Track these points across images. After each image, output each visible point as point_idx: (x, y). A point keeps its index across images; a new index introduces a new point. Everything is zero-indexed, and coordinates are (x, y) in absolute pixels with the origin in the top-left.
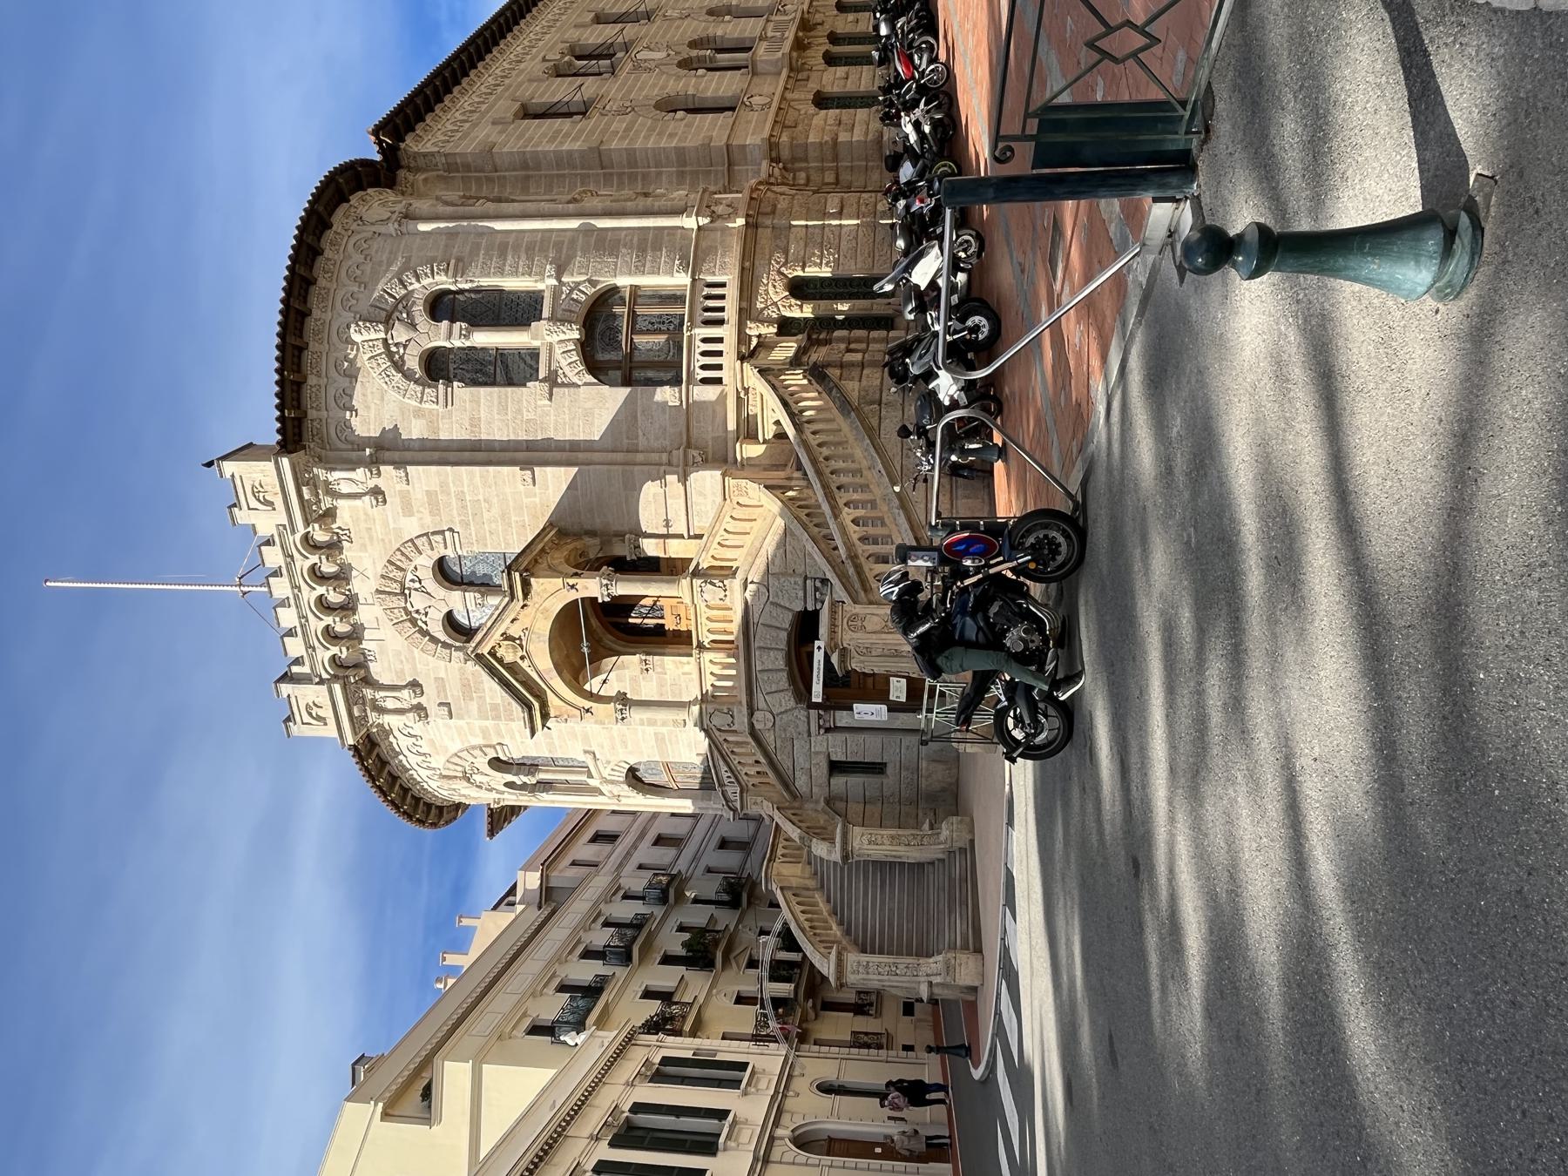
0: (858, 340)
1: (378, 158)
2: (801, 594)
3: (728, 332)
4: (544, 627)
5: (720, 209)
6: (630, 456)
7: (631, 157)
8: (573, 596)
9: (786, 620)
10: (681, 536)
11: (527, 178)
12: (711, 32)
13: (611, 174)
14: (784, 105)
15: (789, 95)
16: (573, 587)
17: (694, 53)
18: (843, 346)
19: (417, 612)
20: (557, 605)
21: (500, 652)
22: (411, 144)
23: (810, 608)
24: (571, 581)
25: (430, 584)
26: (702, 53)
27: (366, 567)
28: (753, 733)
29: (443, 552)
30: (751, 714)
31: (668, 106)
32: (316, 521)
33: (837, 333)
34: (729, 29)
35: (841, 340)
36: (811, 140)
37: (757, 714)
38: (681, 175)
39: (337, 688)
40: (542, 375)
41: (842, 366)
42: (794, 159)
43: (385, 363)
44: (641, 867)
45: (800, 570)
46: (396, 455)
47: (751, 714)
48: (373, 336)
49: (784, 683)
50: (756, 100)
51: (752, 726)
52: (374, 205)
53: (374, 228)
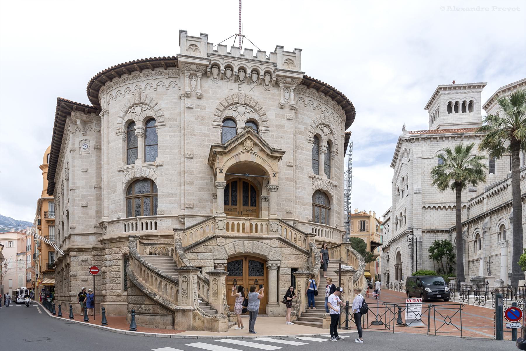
2: (275, 259)
4: (258, 161)
8: (271, 175)
16: (274, 175)
20: (267, 167)
23: (270, 262)
27: (254, 92)
28: (215, 237)
30: (224, 237)
37: (223, 240)
45: (283, 259)
47: (224, 237)
51: (219, 237)
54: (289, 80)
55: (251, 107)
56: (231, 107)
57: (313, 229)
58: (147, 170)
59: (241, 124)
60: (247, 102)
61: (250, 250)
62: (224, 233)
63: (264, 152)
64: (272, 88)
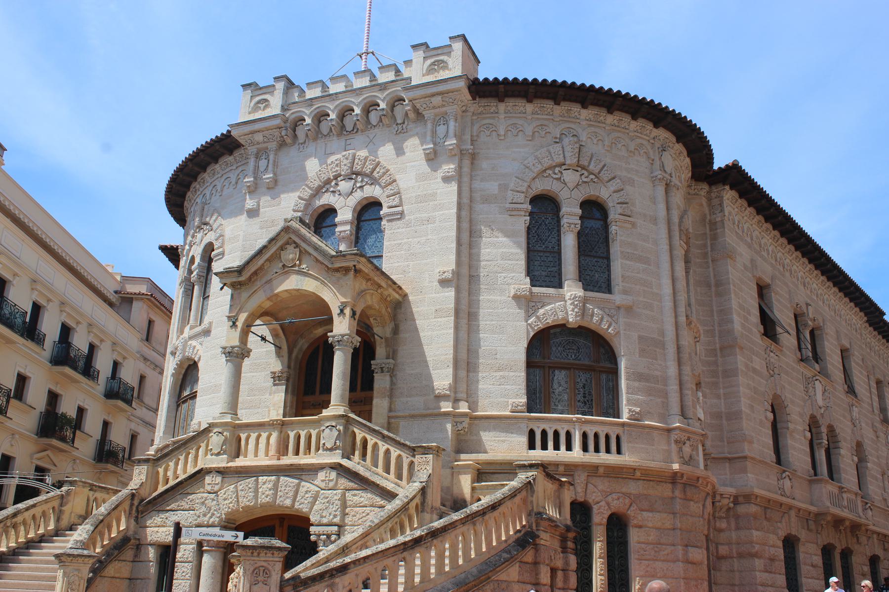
0: (566, 579)
1: (716, 167)
2: (325, 521)
3: (576, 454)
5: (687, 449)
6: (463, 365)
7: (730, 373)
8: (335, 311)
9: (302, 506)
10: (390, 410)
11: (709, 285)
12: (842, 444)
13: (716, 355)
14: (784, 509)
15: (793, 513)
17: (824, 430)
18: (559, 564)
19: (337, 184)
21: (290, 248)
22: (729, 195)
23: (312, 529)
24: (347, 311)
25: (359, 195)
26: (825, 437)
29: (385, 205)
31: (776, 409)
32: (414, 107)
33: (573, 560)
34: (846, 460)
35: (567, 563)
36: (755, 533)
38: (718, 416)
39: (277, 122)
40: (536, 290)
41: (536, 563)
42: (737, 517)
43: (547, 162)
44: (142, 378)
46: (466, 169)
47: (221, 472)
48: (568, 155)
49: (244, 502)
50: (787, 483)
52: (677, 161)
53: (657, 159)
54: (437, 100)
55: (366, 175)
56: (328, 186)
57: (532, 434)
58: (193, 343)
59: (345, 214)
60: (357, 168)
61: (268, 499)
62: (221, 462)
63: (322, 263)
64: (411, 125)
